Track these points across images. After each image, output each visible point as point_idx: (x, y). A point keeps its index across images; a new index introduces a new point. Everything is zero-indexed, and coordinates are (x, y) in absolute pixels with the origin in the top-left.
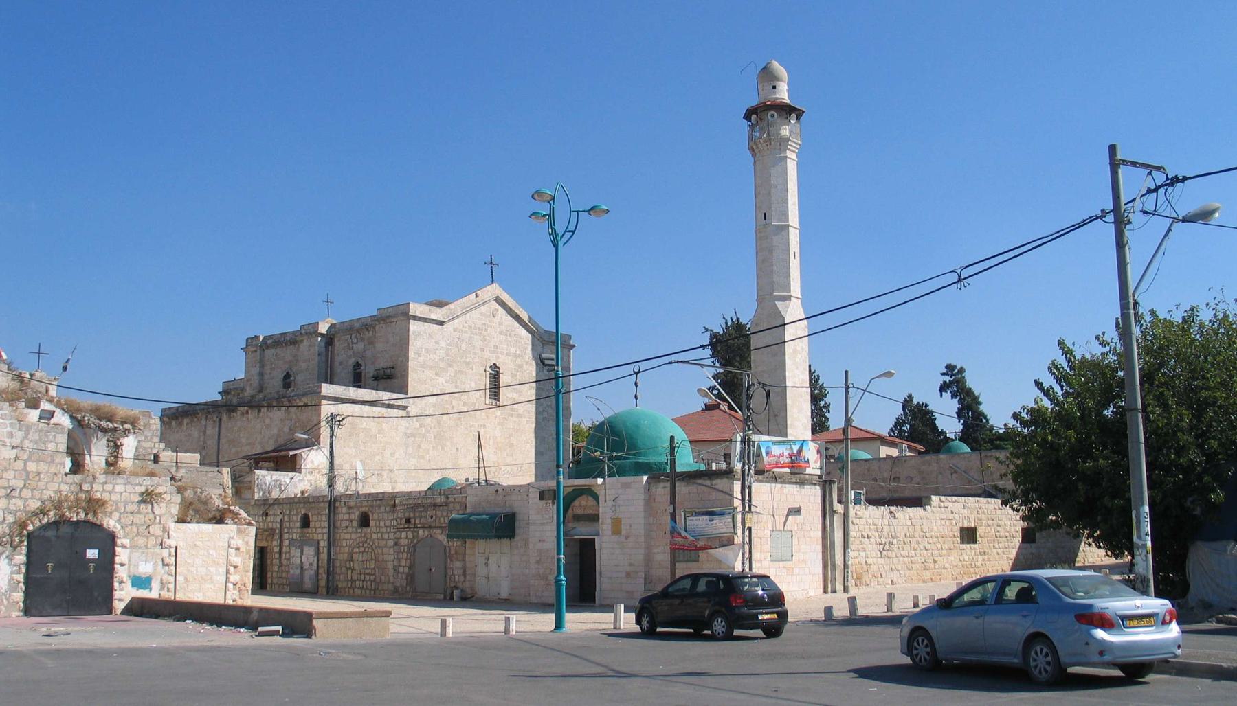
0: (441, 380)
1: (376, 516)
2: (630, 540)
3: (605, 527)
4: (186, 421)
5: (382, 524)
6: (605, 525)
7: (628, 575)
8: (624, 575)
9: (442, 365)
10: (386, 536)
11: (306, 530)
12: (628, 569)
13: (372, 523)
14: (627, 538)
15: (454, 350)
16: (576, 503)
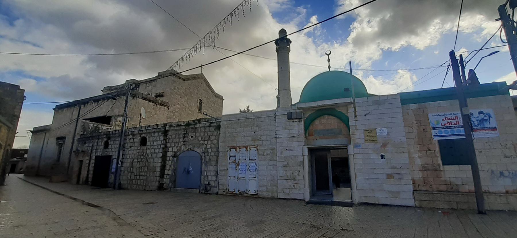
0: (182, 100)
1: (151, 139)
2: (389, 146)
3: (357, 137)
4: (65, 109)
5: (155, 143)
6: (358, 135)
7: (390, 176)
8: (385, 177)
9: (183, 95)
10: (157, 151)
11: (105, 150)
12: (390, 171)
13: (148, 143)
14: (384, 145)
15: (188, 91)
16: (317, 122)
